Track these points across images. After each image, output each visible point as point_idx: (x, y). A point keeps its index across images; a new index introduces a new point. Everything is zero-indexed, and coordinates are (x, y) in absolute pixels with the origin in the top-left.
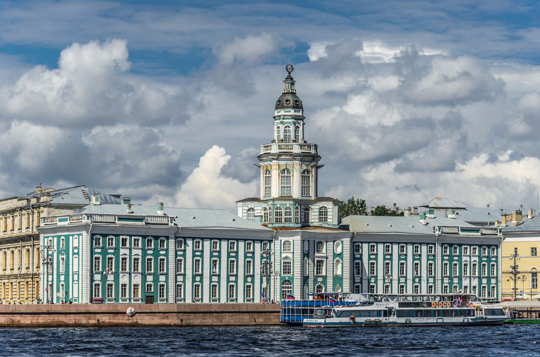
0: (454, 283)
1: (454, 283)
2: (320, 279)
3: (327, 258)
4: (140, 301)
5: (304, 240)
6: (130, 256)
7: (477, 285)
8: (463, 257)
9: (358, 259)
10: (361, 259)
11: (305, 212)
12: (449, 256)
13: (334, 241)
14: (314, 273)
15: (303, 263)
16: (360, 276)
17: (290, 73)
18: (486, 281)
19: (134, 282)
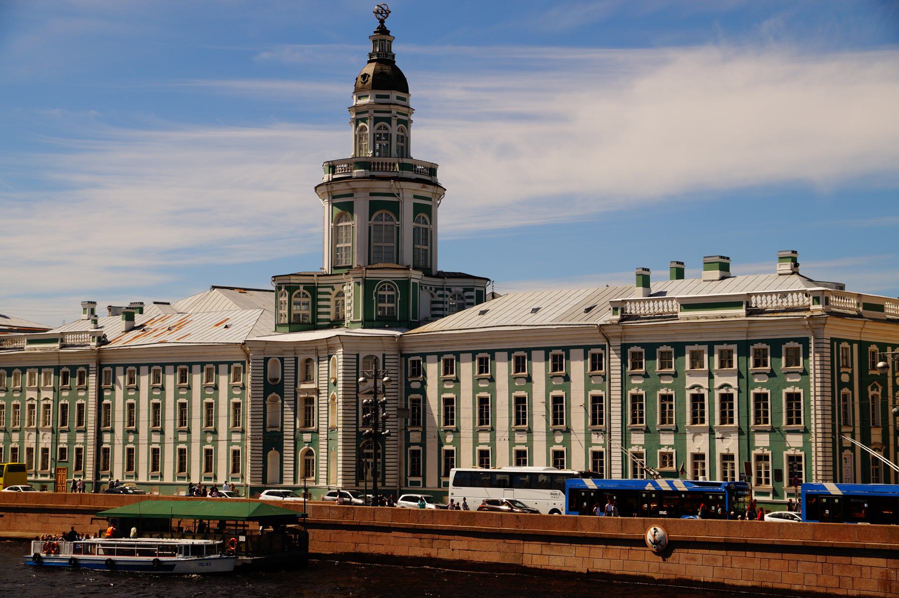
0: (663, 446)
1: (663, 446)
2: (307, 437)
3: (318, 392)
4: (49, 476)
5: (266, 360)
6: (38, 401)
7: (734, 451)
8: (687, 377)
9: (415, 391)
10: (423, 391)
11: (337, 299)
12: (646, 376)
13: (330, 357)
14: (295, 425)
15: (328, 403)
16: (421, 429)
17: (382, 22)
18: (179, 438)
19: (41, 446)
